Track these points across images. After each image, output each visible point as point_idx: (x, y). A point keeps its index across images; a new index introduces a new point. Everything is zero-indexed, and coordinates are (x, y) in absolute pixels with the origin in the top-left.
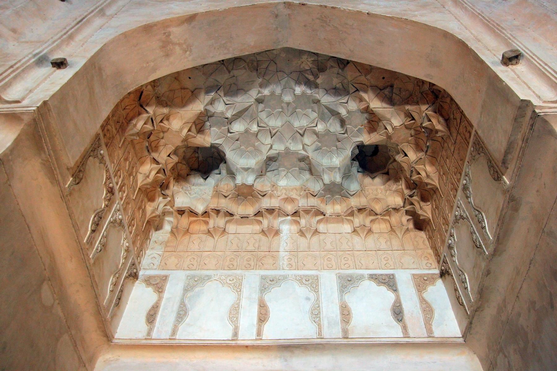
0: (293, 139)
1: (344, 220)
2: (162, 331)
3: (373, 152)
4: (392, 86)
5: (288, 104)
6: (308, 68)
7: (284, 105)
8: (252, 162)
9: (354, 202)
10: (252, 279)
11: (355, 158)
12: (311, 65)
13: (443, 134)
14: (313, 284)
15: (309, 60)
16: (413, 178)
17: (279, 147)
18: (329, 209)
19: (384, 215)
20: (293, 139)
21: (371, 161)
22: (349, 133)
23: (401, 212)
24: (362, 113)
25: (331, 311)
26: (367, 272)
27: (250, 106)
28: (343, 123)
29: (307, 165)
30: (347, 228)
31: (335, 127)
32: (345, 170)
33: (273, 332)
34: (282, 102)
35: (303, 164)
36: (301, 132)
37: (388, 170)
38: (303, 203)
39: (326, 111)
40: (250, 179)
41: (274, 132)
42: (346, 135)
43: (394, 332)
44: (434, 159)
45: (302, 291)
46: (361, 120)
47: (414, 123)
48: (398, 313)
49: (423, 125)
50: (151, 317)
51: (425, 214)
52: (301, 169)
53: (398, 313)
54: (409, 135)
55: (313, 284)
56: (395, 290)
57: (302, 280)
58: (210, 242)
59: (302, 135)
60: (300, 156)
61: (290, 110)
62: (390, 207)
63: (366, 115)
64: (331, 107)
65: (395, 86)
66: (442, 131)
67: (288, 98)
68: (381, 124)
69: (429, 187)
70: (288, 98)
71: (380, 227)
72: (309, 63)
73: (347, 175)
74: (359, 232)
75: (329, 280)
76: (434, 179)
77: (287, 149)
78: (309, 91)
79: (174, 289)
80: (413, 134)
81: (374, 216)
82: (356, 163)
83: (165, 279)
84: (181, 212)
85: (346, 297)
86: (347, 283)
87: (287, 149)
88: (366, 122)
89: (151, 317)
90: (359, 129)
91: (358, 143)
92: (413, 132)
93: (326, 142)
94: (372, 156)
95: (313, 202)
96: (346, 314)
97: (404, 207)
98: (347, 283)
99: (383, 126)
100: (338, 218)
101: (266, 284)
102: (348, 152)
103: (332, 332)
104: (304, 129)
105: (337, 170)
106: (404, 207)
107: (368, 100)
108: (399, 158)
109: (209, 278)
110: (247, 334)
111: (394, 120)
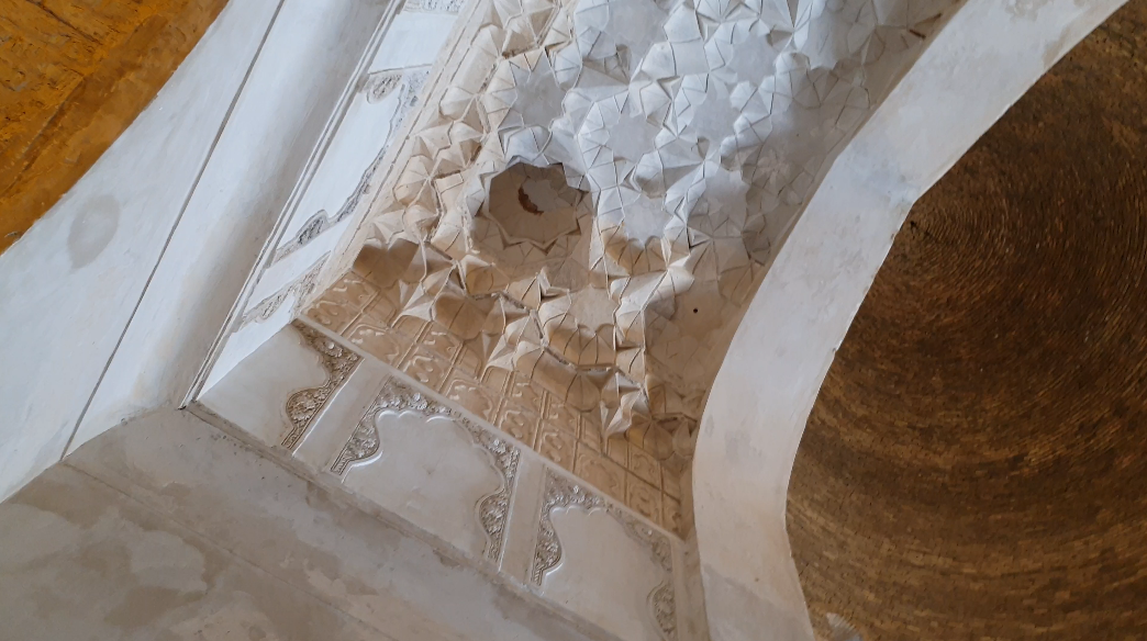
0: (666, 57)
1: (469, 96)
3: (527, 196)
4: (672, 318)
5: (730, 88)
6: (760, 163)
7: (733, 78)
11: (555, 173)
12: (763, 171)
13: (604, 419)
15: (774, 174)
16: (502, 300)
19: (427, 192)
20: (666, 57)
21: (533, 204)
22: (623, 190)
23: (418, 235)
24: (651, 238)
27: (793, 18)
28: (645, 184)
29: (607, 65)
31: (647, 166)
32: (561, 146)
34: (741, 79)
35: (609, 50)
36: (669, 85)
37: (485, 218)
39: (683, 163)
41: (706, 25)
42: (621, 180)
44: (539, 366)
46: (638, 229)
47: (610, 346)
49: (617, 374)
51: (413, 299)
52: (599, 39)
54: (582, 323)
59: (661, 82)
60: (633, 56)
61: (718, 85)
62: (443, 214)
63: (642, 242)
64: (686, 178)
65: (669, 323)
66: (610, 417)
68: (624, 272)
69: (403, 287)
70: (740, 92)
72: (768, 170)
73: (546, 141)
74: (437, 129)
76: (416, 308)
77: (664, 37)
78: (726, 140)
80: (584, 331)
81: (439, 169)
82: (540, 161)
87: (664, 37)
88: (628, 235)
90: (621, 215)
91: (595, 198)
92: (590, 333)
94: (521, 191)
97: (428, 244)
99: (616, 274)
102: (593, 172)
104: (672, 95)
105: (571, 130)
106: (428, 244)
107: (674, 264)
108: (542, 280)
111: (631, 304)
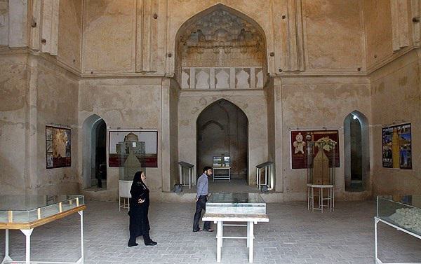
2: (192, 87)
8: (210, 33)
9: (241, 44)
10: (212, 69)
14: (228, 71)
17: (218, 27)
18: (234, 45)
25: (233, 80)
26: (243, 67)
30: (239, 50)
33: (218, 87)
38: (226, 44)
40: (210, 38)
43: (247, 87)
45: (225, 74)
48: (249, 81)
50: (189, 83)
53: (249, 81)
55: (228, 71)
56: (249, 74)
57: (226, 70)
58: (199, 55)
67: (221, 14)
71: (250, 49)
75: (233, 70)
79: (193, 70)
83: (189, 70)
84: (189, 47)
85: (237, 76)
86: (237, 71)
89: (189, 83)
93: (233, 27)
95: (229, 43)
96: (236, 80)
98: (237, 71)
100: (236, 47)
101: (217, 71)
103: (233, 87)
109: (201, 70)
110: (213, 87)
